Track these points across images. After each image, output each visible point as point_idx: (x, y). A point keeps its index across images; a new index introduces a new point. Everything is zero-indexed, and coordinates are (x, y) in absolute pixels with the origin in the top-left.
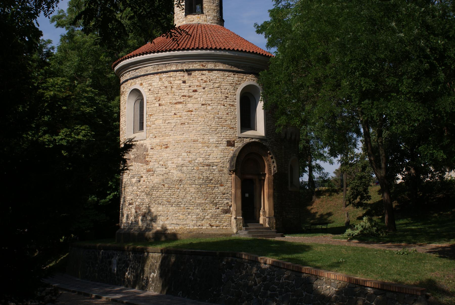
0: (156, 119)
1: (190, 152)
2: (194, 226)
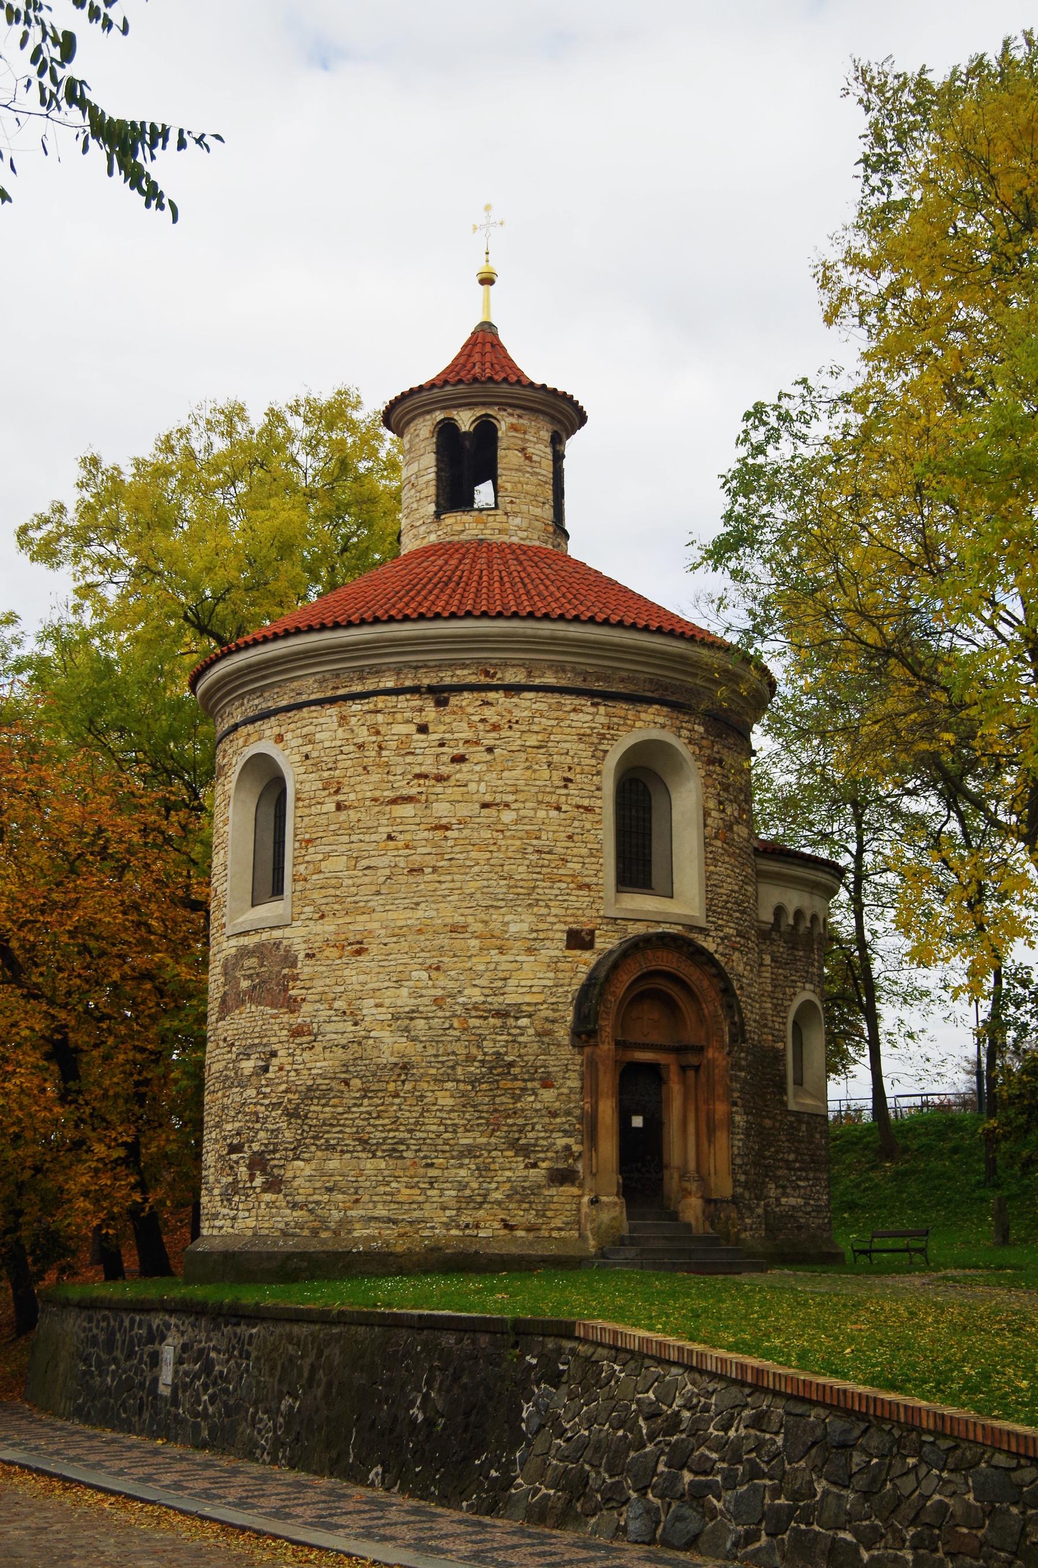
0: (327, 856)
1: (438, 969)
2: (447, 1226)
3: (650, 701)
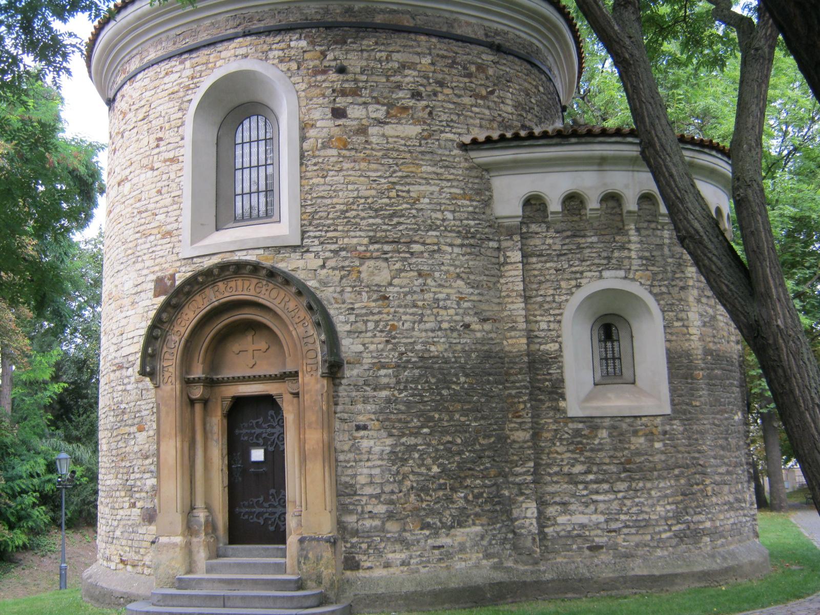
3: (230, 39)
